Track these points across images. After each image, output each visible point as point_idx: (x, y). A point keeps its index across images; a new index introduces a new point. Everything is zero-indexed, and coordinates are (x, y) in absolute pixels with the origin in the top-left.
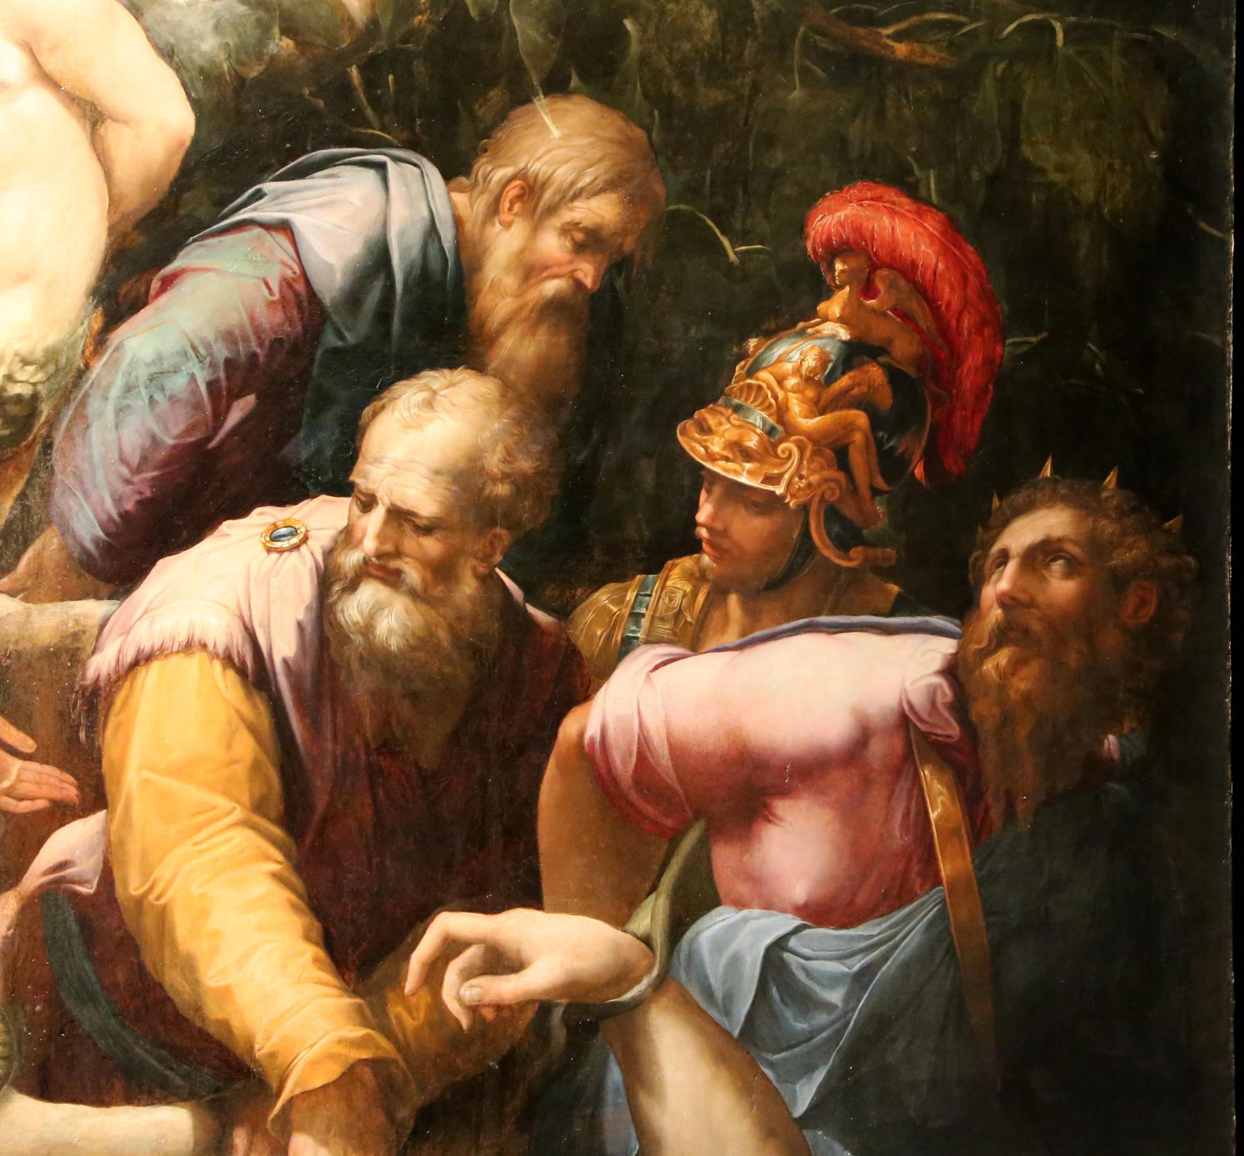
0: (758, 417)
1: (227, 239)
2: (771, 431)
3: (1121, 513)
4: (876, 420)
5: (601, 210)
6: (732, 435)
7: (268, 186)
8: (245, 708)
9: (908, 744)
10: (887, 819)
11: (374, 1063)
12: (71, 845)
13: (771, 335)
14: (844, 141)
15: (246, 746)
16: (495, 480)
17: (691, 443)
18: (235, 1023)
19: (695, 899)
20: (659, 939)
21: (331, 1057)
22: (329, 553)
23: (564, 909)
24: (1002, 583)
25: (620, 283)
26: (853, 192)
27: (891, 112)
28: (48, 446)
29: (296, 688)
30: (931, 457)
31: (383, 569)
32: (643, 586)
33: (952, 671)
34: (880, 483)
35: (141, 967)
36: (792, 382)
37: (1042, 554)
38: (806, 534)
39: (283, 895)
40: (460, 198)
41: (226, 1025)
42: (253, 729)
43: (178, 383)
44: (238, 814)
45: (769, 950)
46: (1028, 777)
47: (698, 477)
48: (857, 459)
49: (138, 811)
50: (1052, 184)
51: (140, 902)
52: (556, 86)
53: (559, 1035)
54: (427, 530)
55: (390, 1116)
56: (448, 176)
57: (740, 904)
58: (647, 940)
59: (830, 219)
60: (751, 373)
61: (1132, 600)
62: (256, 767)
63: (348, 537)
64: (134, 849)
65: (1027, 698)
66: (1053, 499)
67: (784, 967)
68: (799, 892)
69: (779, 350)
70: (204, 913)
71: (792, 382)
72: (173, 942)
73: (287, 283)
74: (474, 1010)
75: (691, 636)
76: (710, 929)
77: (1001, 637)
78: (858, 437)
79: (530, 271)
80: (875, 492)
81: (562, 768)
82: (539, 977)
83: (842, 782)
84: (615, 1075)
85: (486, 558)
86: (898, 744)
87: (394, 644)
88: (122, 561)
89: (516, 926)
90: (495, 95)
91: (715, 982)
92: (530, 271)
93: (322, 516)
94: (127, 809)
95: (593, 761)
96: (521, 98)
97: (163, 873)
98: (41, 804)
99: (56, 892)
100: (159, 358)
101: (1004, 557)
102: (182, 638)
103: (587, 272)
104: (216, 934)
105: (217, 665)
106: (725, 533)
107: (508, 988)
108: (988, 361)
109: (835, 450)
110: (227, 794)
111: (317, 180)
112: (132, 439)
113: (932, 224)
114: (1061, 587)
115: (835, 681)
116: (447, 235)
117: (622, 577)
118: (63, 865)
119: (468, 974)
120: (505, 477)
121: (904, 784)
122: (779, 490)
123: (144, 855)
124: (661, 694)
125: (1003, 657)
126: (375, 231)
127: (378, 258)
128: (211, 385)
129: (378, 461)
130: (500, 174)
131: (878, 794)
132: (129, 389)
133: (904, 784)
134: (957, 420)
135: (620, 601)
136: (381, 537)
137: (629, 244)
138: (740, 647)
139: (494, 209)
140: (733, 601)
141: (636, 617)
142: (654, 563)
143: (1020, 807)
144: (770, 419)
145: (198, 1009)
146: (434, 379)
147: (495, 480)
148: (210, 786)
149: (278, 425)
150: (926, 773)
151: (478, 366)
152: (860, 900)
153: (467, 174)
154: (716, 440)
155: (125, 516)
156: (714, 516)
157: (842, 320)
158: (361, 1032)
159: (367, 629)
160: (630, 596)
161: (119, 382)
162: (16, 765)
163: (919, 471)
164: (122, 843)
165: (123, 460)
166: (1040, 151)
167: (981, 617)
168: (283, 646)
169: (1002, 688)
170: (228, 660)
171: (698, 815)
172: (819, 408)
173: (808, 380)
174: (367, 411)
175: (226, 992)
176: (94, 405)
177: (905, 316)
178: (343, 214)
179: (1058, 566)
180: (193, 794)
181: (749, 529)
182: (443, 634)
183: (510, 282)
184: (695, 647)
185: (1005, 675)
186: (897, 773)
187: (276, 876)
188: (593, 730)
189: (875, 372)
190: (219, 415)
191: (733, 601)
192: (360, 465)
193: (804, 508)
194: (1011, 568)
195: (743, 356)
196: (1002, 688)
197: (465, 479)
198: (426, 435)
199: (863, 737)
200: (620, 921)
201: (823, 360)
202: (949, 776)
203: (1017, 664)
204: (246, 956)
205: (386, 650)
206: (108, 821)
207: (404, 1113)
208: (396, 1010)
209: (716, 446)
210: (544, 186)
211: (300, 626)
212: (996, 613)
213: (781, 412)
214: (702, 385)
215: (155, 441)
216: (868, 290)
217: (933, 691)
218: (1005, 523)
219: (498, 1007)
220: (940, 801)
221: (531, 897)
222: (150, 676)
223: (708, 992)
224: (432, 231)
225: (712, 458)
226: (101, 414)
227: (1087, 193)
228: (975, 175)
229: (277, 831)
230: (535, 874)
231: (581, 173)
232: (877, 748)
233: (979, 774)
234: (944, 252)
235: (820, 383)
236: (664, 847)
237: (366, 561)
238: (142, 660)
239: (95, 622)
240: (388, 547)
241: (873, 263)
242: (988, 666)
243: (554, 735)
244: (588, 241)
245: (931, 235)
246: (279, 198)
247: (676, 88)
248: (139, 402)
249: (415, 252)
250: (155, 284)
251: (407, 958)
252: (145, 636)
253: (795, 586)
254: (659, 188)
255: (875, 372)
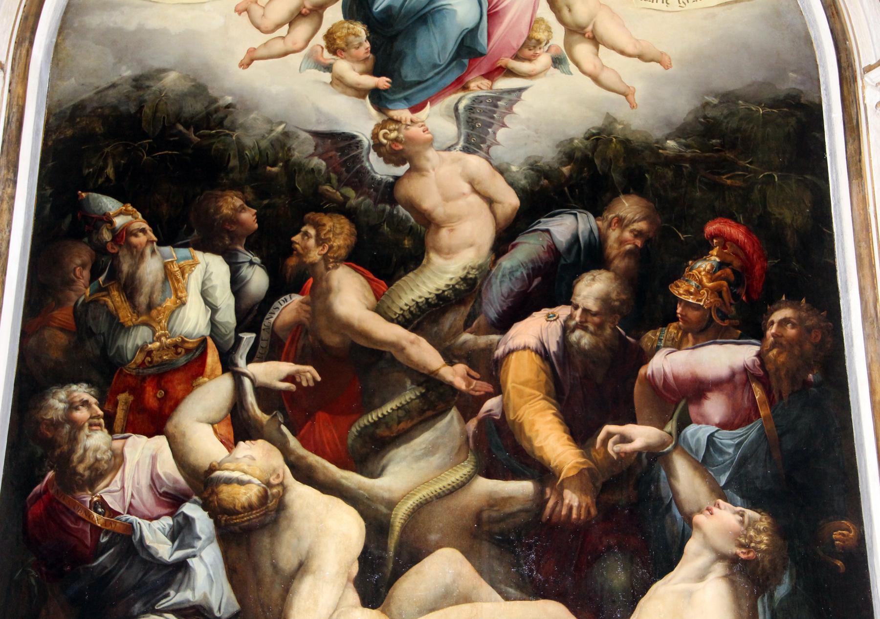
0: (694, 283)
1: (531, 234)
2: (698, 287)
3: (807, 311)
4: (730, 284)
5: (642, 225)
6: (686, 288)
7: (542, 220)
8: (542, 366)
9: (747, 377)
10: (743, 399)
11: (589, 469)
12: (492, 404)
13: (696, 260)
14: (714, 207)
15: (543, 376)
16: (614, 301)
17: (675, 291)
18: (544, 457)
19: (684, 422)
20: (674, 433)
21: (575, 467)
22: (565, 322)
23: (643, 424)
24: (773, 330)
25: (649, 246)
26: (718, 220)
27: (727, 199)
28: (480, 291)
29: (558, 360)
30: (748, 294)
31: (582, 326)
32: (662, 331)
33: (759, 355)
34: (733, 302)
35: (515, 441)
36: (703, 273)
37: (783, 322)
38: (711, 316)
39: (556, 419)
40: (599, 223)
41: (542, 457)
42: (545, 372)
43: (518, 274)
44: (542, 396)
45: (709, 437)
46: (786, 387)
47: (676, 300)
48: (725, 295)
49: (512, 395)
50: (777, 219)
51: (514, 421)
52: (626, 192)
53: (645, 461)
54: (595, 314)
55: (594, 484)
56: (595, 217)
57: (698, 423)
58: (670, 434)
59: (711, 228)
60: (691, 270)
61: (813, 335)
62: (547, 382)
63: (571, 317)
64: (511, 406)
65: (783, 363)
66: (786, 307)
67: (714, 442)
68: (717, 419)
69: (698, 264)
70: (533, 425)
71: (703, 273)
72: (524, 433)
73: (549, 247)
74: (618, 454)
75: (678, 346)
76: (690, 430)
77: (774, 345)
78: (725, 289)
79: (621, 242)
80: (731, 304)
81: (640, 383)
82: (638, 444)
83: (728, 388)
84: (663, 473)
85: (613, 323)
86: (744, 376)
87: (587, 347)
88: (503, 324)
89: (629, 429)
90: (608, 195)
91: (693, 446)
92: (621, 242)
93: (563, 311)
94: (509, 394)
95: (650, 381)
96: (616, 195)
97: (520, 413)
98: (482, 393)
99: (489, 416)
100: (512, 267)
101: (772, 323)
102: (522, 345)
103: (639, 243)
104: (537, 431)
105: (533, 353)
106: (686, 316)
107: (628, 447)
108: (763, 268)
109: (718, 292)
110: (538, 390)
111: (557, 218)
112: (505, 289)
113: (742, 229)
114: (791, 332)
115: (723, 358)
116: (596, 233)
117: (655, 328)
118: (490, 410)
119: (615, 443)
120: (617, 300)
121: (747, 388)
122: (702, 304)
123: (514, 408)
124: (668, 362)
125: (775, 351)
126: (574, 232)
127: (576, 238)
128: (528, 275)
129: (579, 295)
130: (611, 216)
131: (739, 393)
132: (503, 276)
133: (747, 388)
134: (754, 284)
135: (655, 335)
136: (581, 317)
137: (651, 235)
138: (693, 348)
139: (610, 226)
140: (690, 335)
141: (660, 340)
142: (665, 324)
143: (784, 395)
144: (698, 282)
145: (533, 453)
146: (595, 273)
147: (614, 301)
148: (533, 388)
149: (548, 285)
150: (753, 385)
151: (607, 269)
152: (736, 422)
153: (601, 216)
154: (681, 290)
155: (503, 311)
156: (682, 311)
157: (717, 256)
158: (583, 460)
159: (578, 343)
160: (658, 334)
161: (500, 274)
162: (475, 382)
163: (744, 298)
164: (507, 404)
165: (502, 295)
166: (773, 209)
167: (767, 340)
168: (553, 348)
169: (775, 360)
170: (536, 352)
171: (683, 397)
172: (711, 280)
173: (708, 272)
174: (575, 282)
175: (541, 447)
176: (493, 280)
177: (737, 255)
178: (563, 227)
179: (789, 325)
180: (528, 390)
181: (693, 315)
182: (601, 345)
183: (616, 245)
184: (679, 348)
185: (776, 357)
186: (744, 385)
187: (554, 414)
188: (649, 372)
189: (728, 271)
190: (530, 284)
191: (690, 335)
192: (573, 297)
193: (710, 309)
194: (775, 326)
195: (688, 266)
196: (775, 360)
197: (605, 300)
198: (592, 289)
199: (733, 374)
200: (662, 427)
201: (712, 267)
202: (761, 386)
203: (779, 353)
204: (546, 438)
205: (584, 349)
206: (503, 398)
207: (599, 484)
208: (593, 453)
209: (681, 292)
210: (624, 219)
211: (558, 342)
212: (772, 339)
213: (700, 282)
214: (677, 273)
215: (512, 290)
216: (724, 247)
217: (754, 361)
218: (772, 313)
219: (625, 453)
220: (758, 393)
221: (634, 421)
222: (513, 357)
223: (691, 449)
224: (591, 231)
225: (680, 294)
226: (495, 283)
227: (788, 221)
228: (754, 216)
229: (554, 401)
230: (635, 415)
231: (635, 215)
232: (737, 377)
233: (770, 386)
234: (746, 237)
235: (712, 274)
236: (674, 406)
237: (577, 324)
238: (511, 352)
239: (496, 341)
240: (583, 320)
241: (725, 240)
242: (771, 354)
243: (637, 373)
244: (638, 234)
245: (743, 234)
246: (546, 223)
247: (662, 192)
248: (507, 280)
249: (587, 237)
250: (510, 247)
251: (596, 438)
252: (511, 345)
253: (707, 331)
254: (659, 220)
255: (728, 271)
